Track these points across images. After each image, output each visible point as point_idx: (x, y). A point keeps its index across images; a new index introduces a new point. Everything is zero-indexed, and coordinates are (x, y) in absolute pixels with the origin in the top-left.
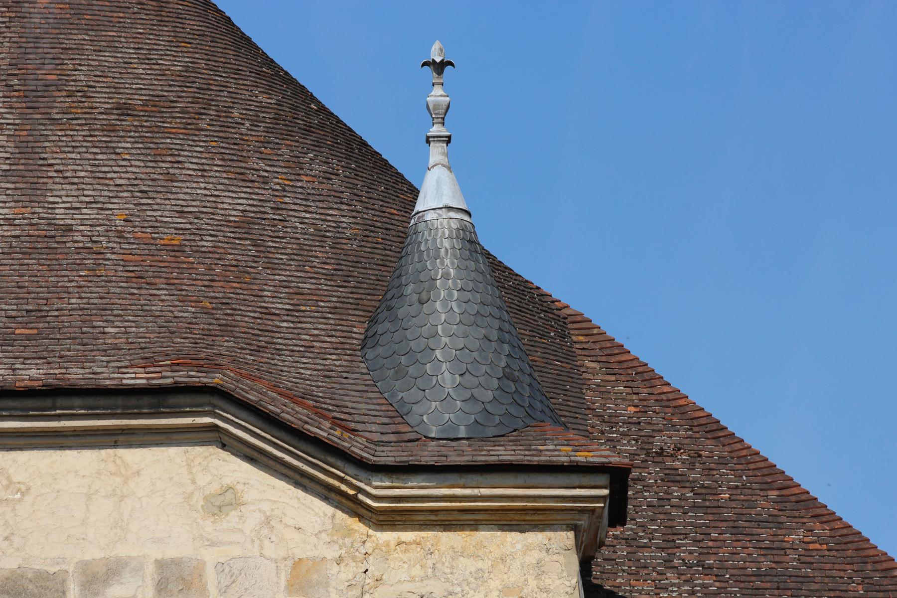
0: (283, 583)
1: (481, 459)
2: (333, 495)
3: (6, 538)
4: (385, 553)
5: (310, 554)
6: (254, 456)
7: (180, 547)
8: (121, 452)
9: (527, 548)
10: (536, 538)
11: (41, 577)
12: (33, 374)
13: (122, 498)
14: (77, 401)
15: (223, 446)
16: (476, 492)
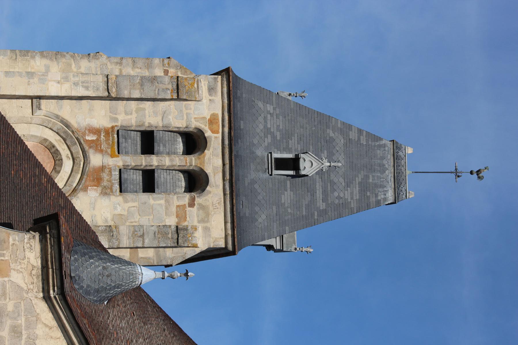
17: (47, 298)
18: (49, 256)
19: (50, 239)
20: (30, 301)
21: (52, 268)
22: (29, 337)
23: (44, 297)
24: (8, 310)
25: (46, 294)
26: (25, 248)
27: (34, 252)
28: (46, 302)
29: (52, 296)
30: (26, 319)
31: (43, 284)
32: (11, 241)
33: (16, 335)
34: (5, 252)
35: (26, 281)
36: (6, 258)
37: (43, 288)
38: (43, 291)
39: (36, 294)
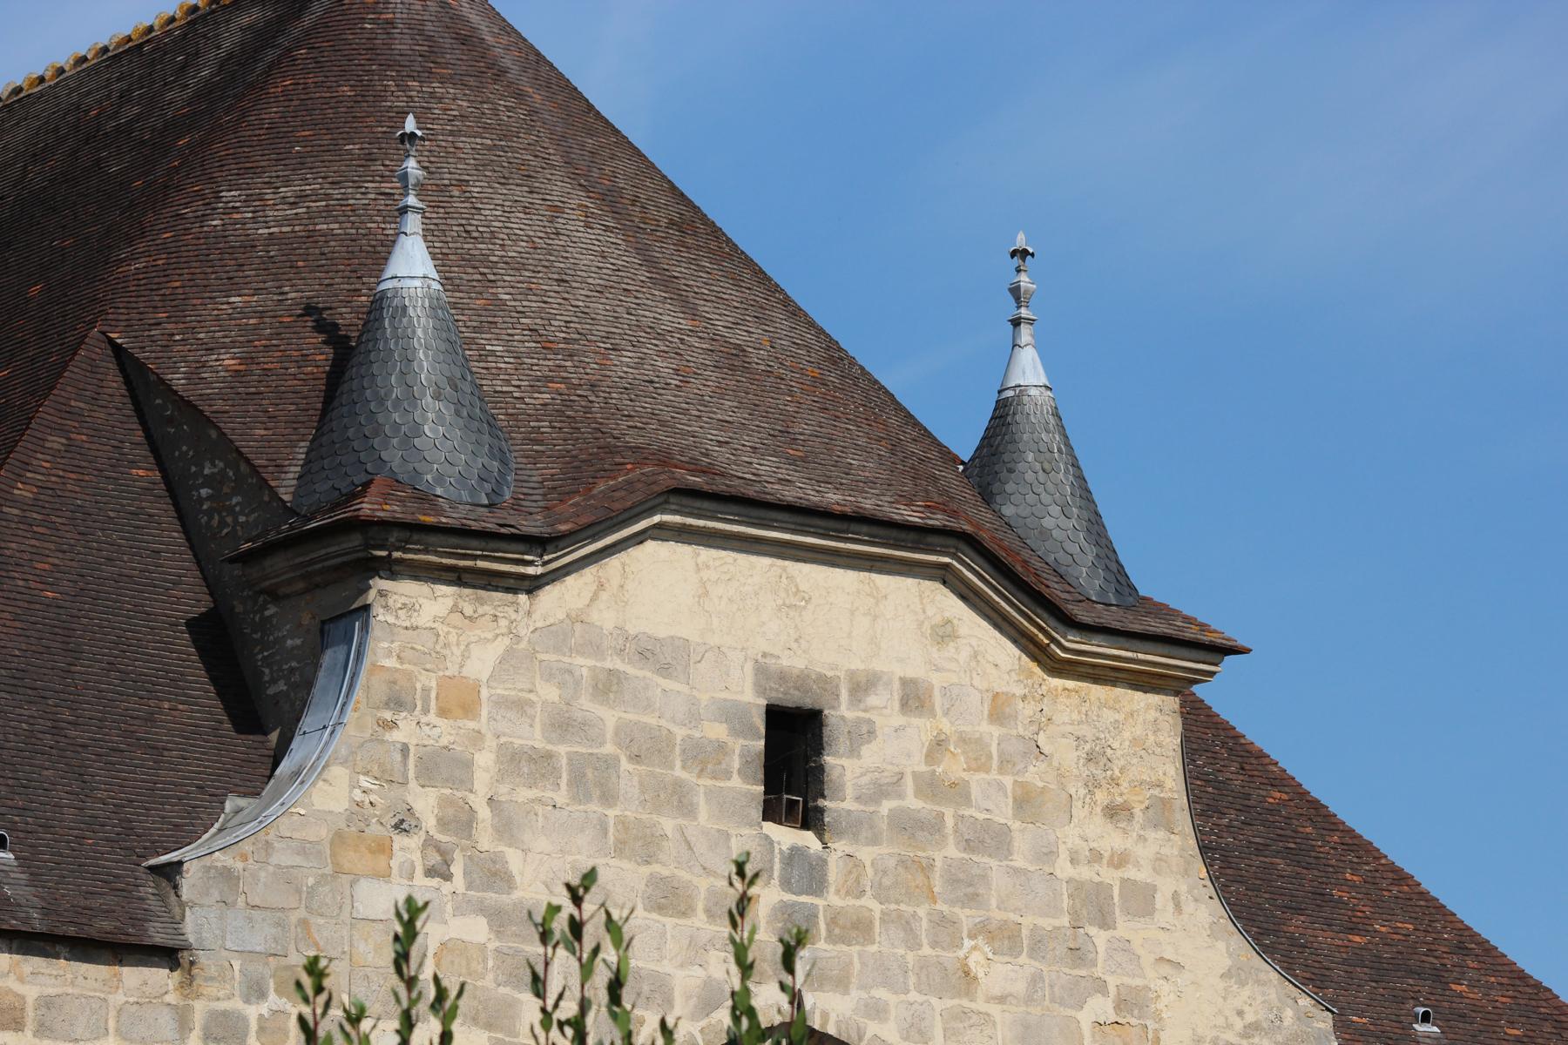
0: (986, 713)
1: (1136, 627)
2: (1024, 641)
3: (796, 641)
4: (1054, 694)
5: (1004, 689)
6: (969, 595)
7: (915, 669)
8: (874, 576)
9: (1148, 707)
10: (1154, 699)
11: (822, 678)
12: (811, 495)
13: (875, 618)
14: (865, 529)
15: (944, 583)
16: (1129, 654)
17: (532, 586)
18: (444, 561)
19: (406, 551)
20: (537, 634)
21: (475, 558)
22: (621, 652)
23: (529, 592)
24: (556, 699)
25: (527, 583)
26: (408, 624)
27: (421, 600)
28: (539, 587)
29: (539, 570)
30: (578, 652)
31: (496, 589)
32: (390, 663)
33: (614, 688)
34: (419, 686)
35: (490, 636)
36: (434, 684)
37: (508, 590)
38: (514, 591)
39: (521, 613)
